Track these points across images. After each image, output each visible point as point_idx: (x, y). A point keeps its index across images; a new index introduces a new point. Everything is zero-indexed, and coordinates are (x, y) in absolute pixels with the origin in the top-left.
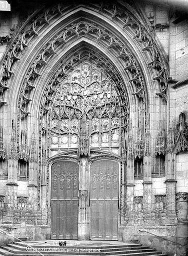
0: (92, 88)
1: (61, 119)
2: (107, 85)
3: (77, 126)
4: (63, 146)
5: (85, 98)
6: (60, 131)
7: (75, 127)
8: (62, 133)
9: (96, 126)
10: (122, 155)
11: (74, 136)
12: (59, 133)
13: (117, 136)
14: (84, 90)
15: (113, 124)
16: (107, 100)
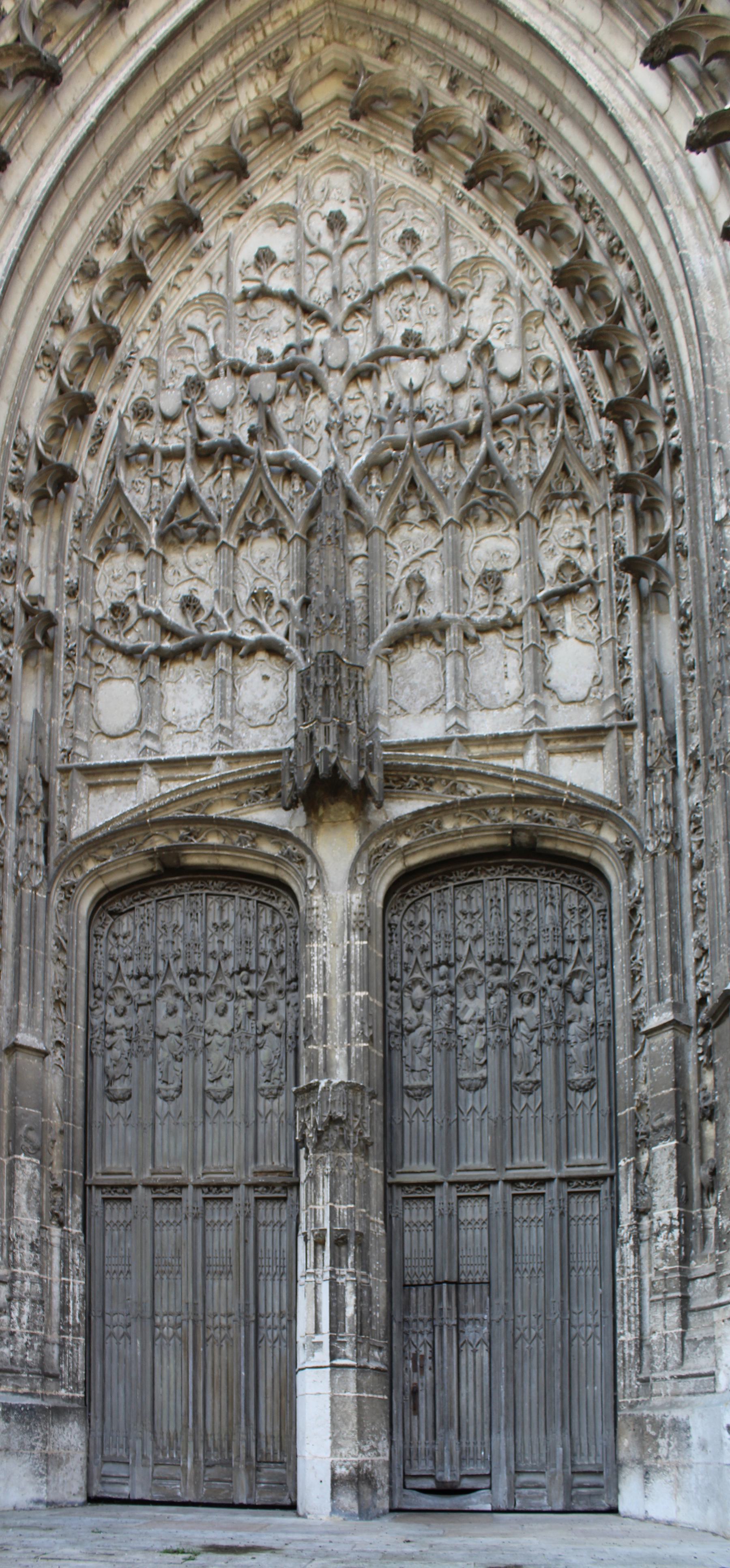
0: (384, 322)
1: (162, 538)
2: (488, 292)
3: (281, 591)
4: (176, 749)
5: (335, 382)
6: (151, 627)
7: (261, 598)
8: (166, 644)
9: (417, 583)
10: (628, 797)
11: (262, 663)
12: (151, 645)
13: (588, 654)
14: (323, 334)
15: (550, 566)
16: (498, 392)
